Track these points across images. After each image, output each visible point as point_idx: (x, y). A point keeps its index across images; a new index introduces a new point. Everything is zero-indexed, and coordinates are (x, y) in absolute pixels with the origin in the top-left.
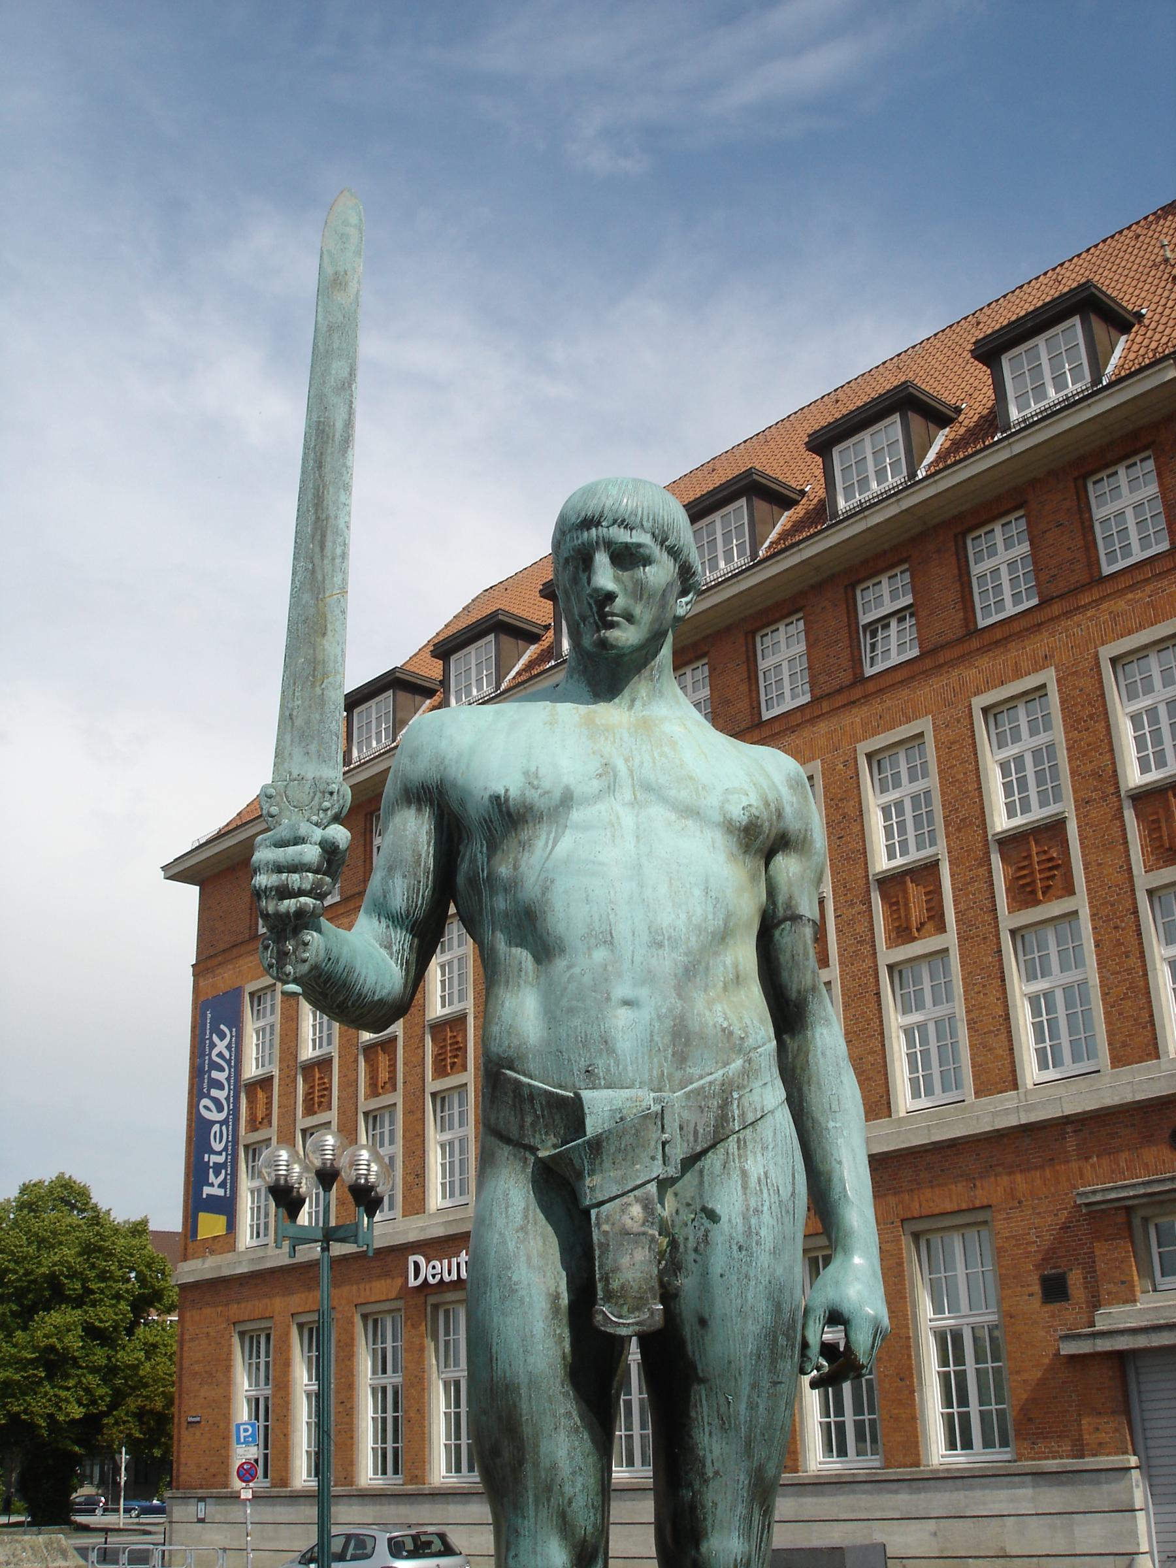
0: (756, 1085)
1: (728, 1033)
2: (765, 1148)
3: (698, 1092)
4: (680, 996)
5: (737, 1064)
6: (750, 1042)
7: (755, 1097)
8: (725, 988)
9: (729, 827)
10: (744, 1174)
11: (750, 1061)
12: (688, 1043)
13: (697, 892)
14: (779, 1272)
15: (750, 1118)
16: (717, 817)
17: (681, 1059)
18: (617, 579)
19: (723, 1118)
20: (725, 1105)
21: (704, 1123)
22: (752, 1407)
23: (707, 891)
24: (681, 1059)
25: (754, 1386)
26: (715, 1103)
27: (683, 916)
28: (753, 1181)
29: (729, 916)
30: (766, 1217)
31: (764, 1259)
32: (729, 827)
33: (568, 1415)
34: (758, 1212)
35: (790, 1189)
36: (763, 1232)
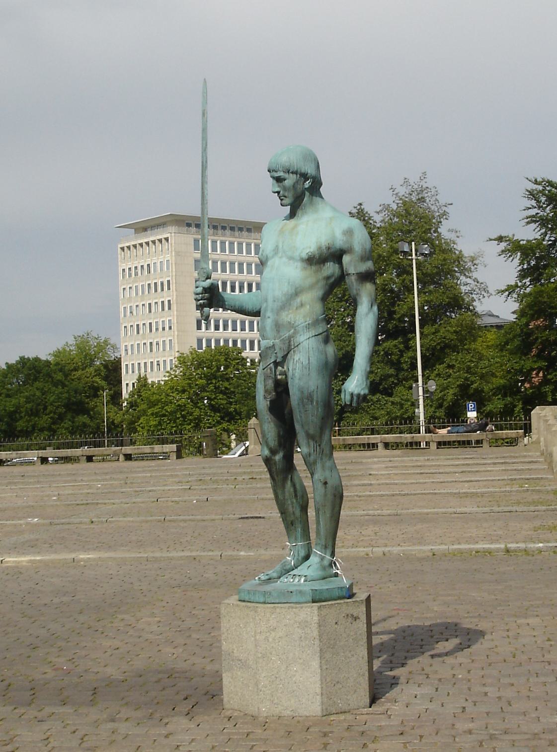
0: (298, 336)
1: (290, 323)
2: (300, 352)
3: (283, 339)
4: (277, 315)
5: (292, 331)
6: (296, 324)
7: (298, 339)
8: (297, 309)
9: (302, 260)
10: (294, 359)
11: (295, 330)
12: (279, 327)
13: (286, 284)
14: (302, 384)
15: (296, 345)
16: (299, 258)
17: (278, 331)
18: (279, 186)
19: (290, 345)
20: (290, 342)
21: (285, 347)
22: (301, 417)
23: (289, 283)
24: (278, 331)
25: (300, 411)
26: (287, 342)
27: (281, 292)
28: (295, 360)
29: (296, 289)
30: (297, 370)
31: (297, 381)
32: (302, 260)
33: (268, 419)
34: (295, 369)
35: (307, 362)
36: (296, 374)
